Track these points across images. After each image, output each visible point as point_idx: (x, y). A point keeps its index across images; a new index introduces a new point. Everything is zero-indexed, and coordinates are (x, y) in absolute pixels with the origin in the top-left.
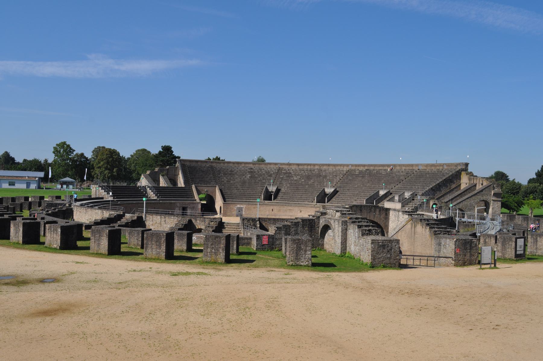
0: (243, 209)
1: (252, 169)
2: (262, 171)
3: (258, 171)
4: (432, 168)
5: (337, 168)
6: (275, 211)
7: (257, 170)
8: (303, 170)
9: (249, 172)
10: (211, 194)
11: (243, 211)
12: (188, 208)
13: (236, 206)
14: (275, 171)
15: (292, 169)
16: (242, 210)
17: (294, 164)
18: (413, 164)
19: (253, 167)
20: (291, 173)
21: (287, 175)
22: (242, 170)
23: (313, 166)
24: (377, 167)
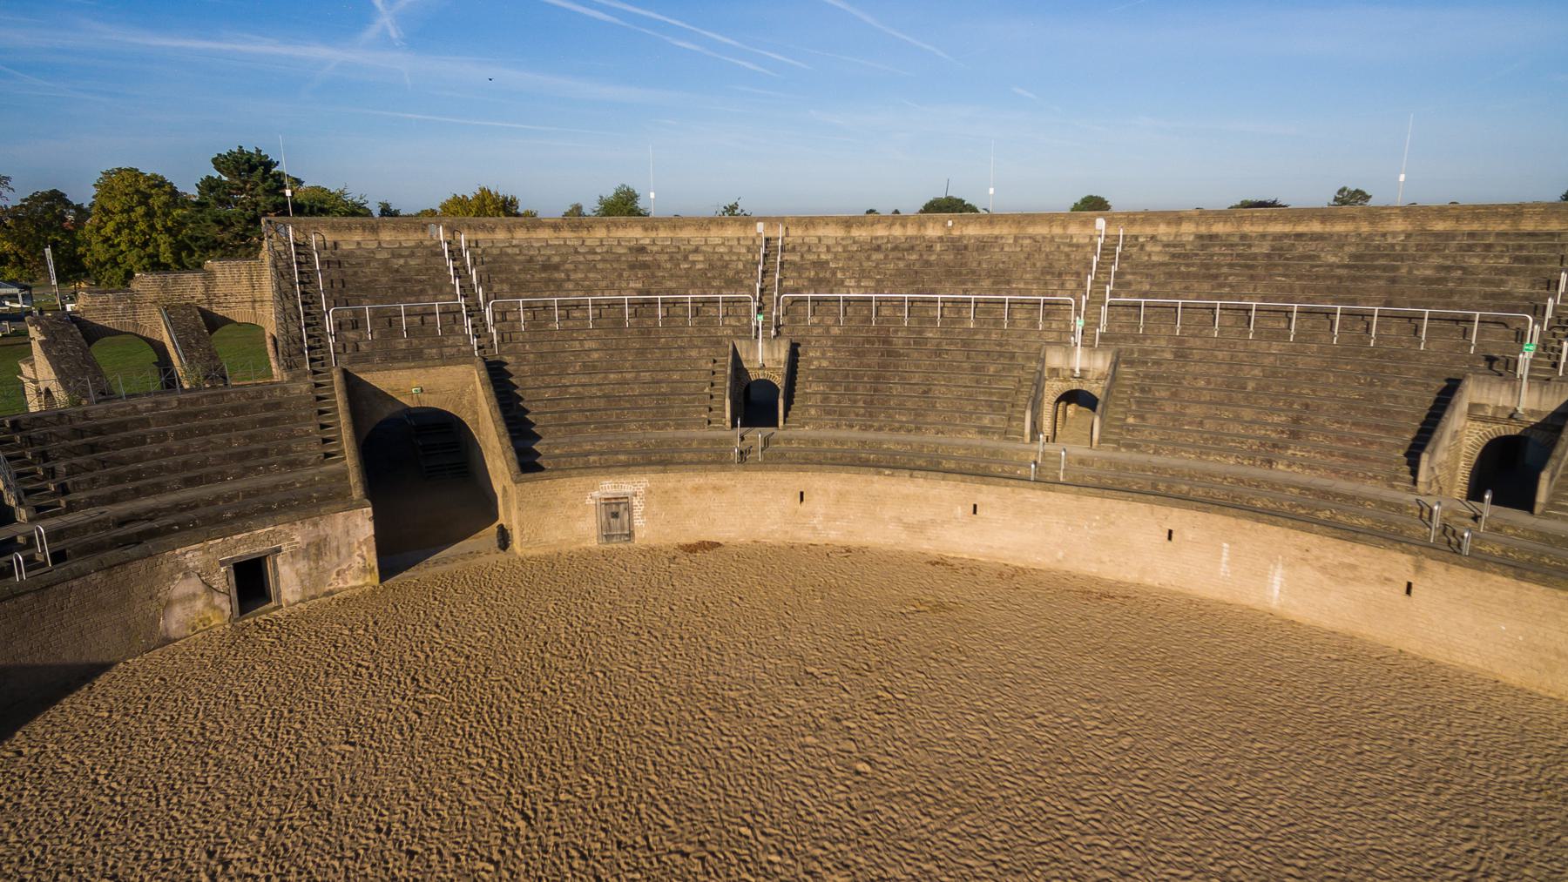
0: (635, 501)
1: (642, 250)
2: (691, 258)
3: (671, 259)
4: (1546, 228)
5: (1040, 230)
6: (817, 505)
7: (666, 257)
8: (878, 248)
9: (632, 267)
10: (449, 409)
11: (637, 513)
12: (279, 560)
13: (593, 489)
14: (750, 257)
15: (825, 241)
16: (629, 509)
17: (826, 221)
18: (1522, 206)
19: (647, 241)
20: (827, 262)
21: (812, 274)
22: (599, 257)
23: (915, 226)
24: (1252, 224)
